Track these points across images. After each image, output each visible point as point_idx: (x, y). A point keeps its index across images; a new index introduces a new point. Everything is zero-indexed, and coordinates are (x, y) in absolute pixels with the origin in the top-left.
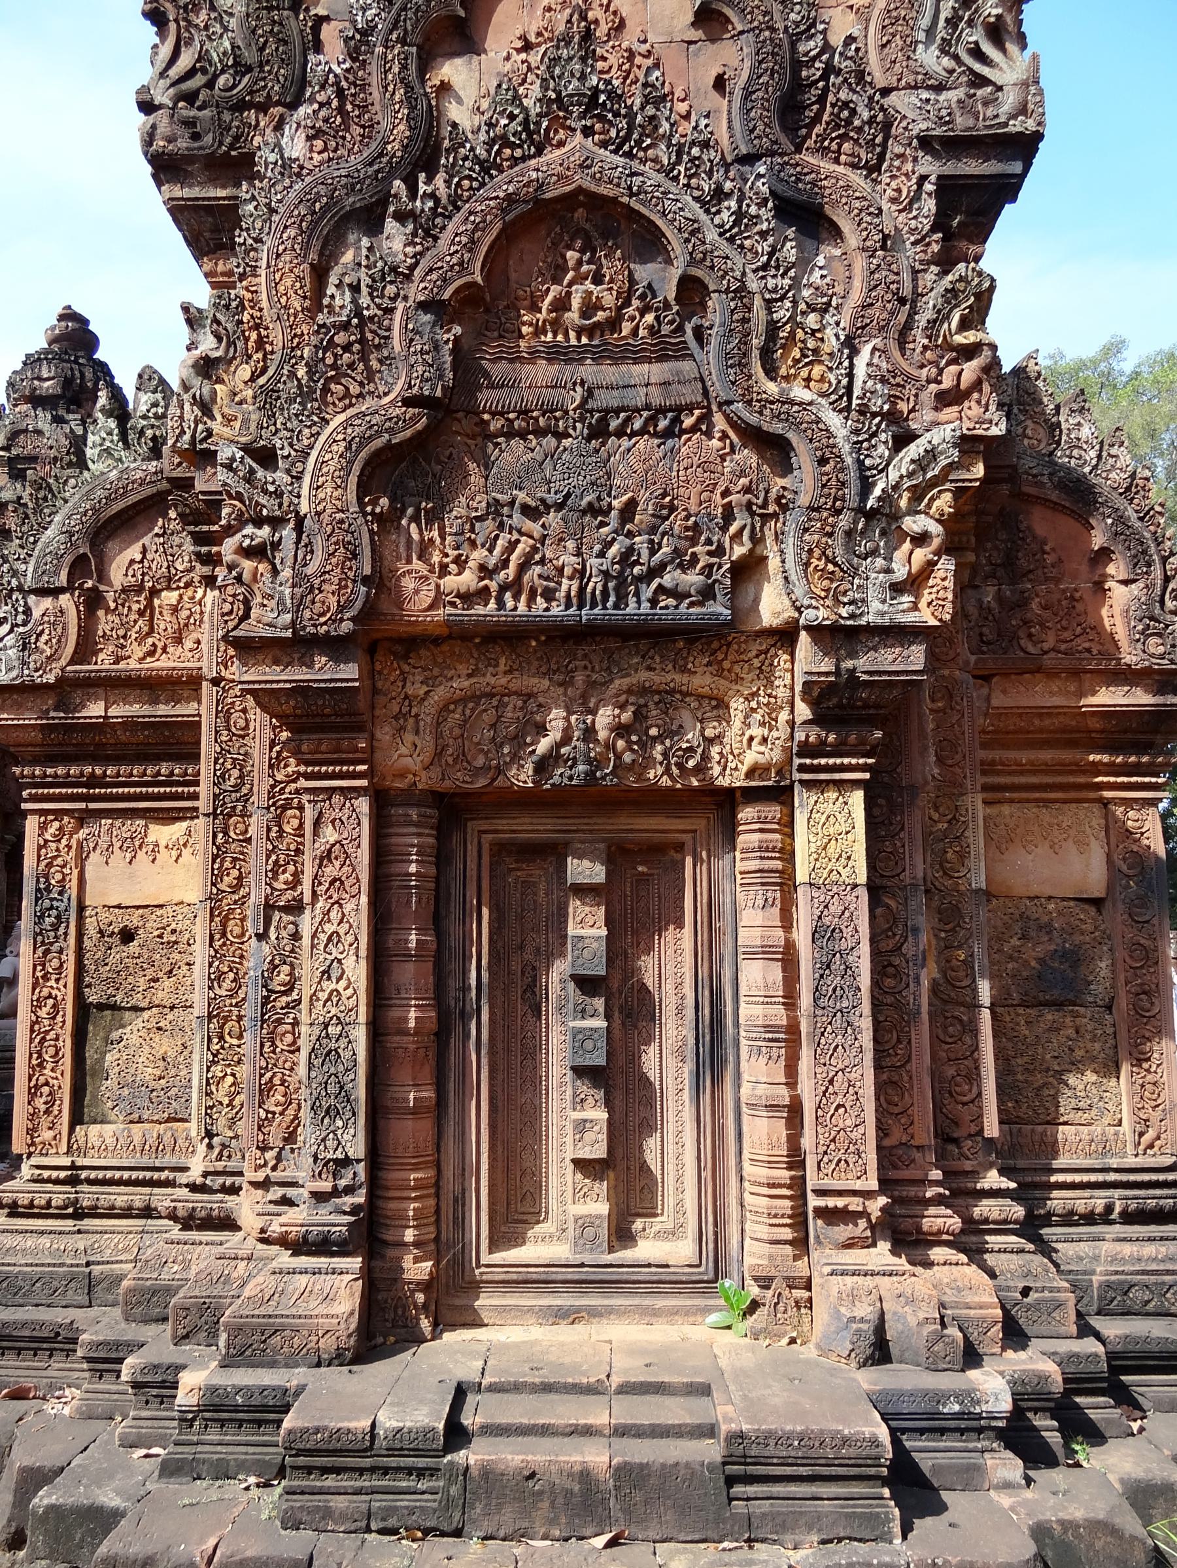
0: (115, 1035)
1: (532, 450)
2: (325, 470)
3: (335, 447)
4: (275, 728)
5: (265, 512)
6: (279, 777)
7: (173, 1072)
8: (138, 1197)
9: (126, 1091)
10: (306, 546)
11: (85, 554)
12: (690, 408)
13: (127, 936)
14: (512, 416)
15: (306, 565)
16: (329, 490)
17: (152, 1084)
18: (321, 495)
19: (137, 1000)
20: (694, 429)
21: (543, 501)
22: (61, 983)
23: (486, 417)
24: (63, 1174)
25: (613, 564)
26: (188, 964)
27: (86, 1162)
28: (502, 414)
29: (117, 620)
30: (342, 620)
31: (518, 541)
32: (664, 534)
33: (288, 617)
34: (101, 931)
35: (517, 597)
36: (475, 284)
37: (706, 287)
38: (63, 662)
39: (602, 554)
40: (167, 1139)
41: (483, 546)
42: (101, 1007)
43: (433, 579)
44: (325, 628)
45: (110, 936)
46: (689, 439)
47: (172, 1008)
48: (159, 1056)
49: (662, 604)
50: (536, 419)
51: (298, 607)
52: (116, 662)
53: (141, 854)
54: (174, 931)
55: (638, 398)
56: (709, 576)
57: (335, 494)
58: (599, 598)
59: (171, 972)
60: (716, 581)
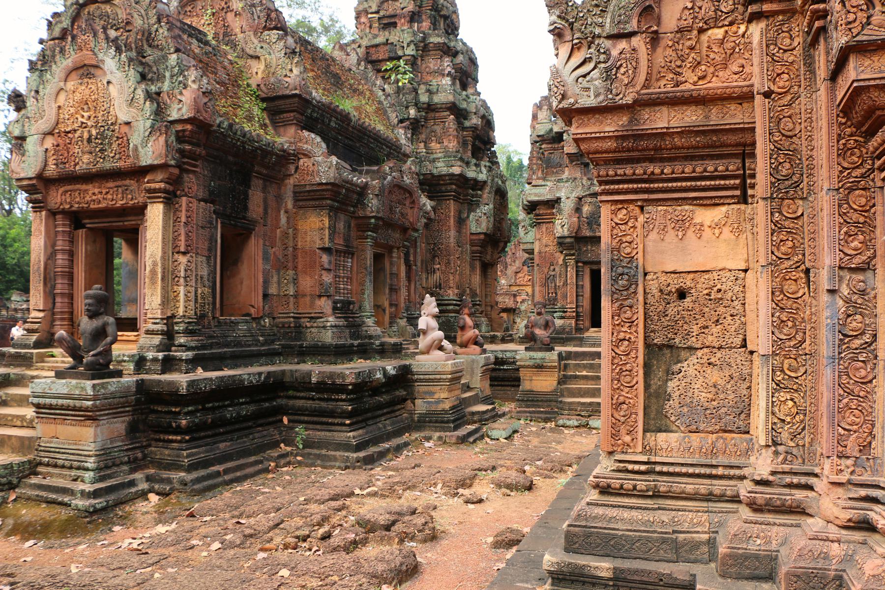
0: (676, 368)
4: (841, 124)
6: (846, 165)
7: (722, 396)
8: (703, 486)
9: (686, 409)
11: (650, 6)
13: (682, 294)
17: (706, 404)
19: (692, 342)
22: (634, 329)
24: (643, 468)
26: (732, 316)
27: (658, 459)
29: (674, 54)
34: (661, 291)
38: (638, 88)
40: (720, 444)
42: (661, 347)
45: (668, 294)
47: (719, 348)
48: (710, 384)
52: (677, 85)
53: (690, 233)
54: (719, 291)
59: (717, 321)
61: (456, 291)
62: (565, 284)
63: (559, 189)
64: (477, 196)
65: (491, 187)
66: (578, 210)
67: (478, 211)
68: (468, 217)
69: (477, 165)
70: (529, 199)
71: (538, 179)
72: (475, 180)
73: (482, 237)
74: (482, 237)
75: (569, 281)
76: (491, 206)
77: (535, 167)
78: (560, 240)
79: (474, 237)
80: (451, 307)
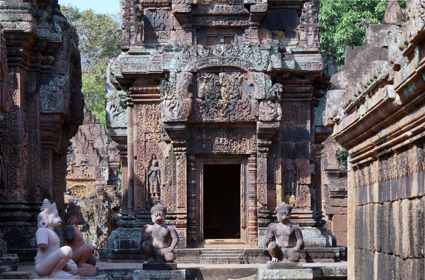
61: (24, 191)
62: (173, 183)
63: (167, 60)
64: (47, 62)
65: (68, 51)
66: (192, 88)
67: (51, 83)
68: (37, 90)
69: (50, 20)
70: (125, 71)
71: (137, 44)
72: (50, 43)
73: (57, 118)
74: (57, 118)
75: (178, 179)
76: (68, 77)
77: (133, 28)
78: (169, 127)
79: (45, 119)
80: (19, 213)
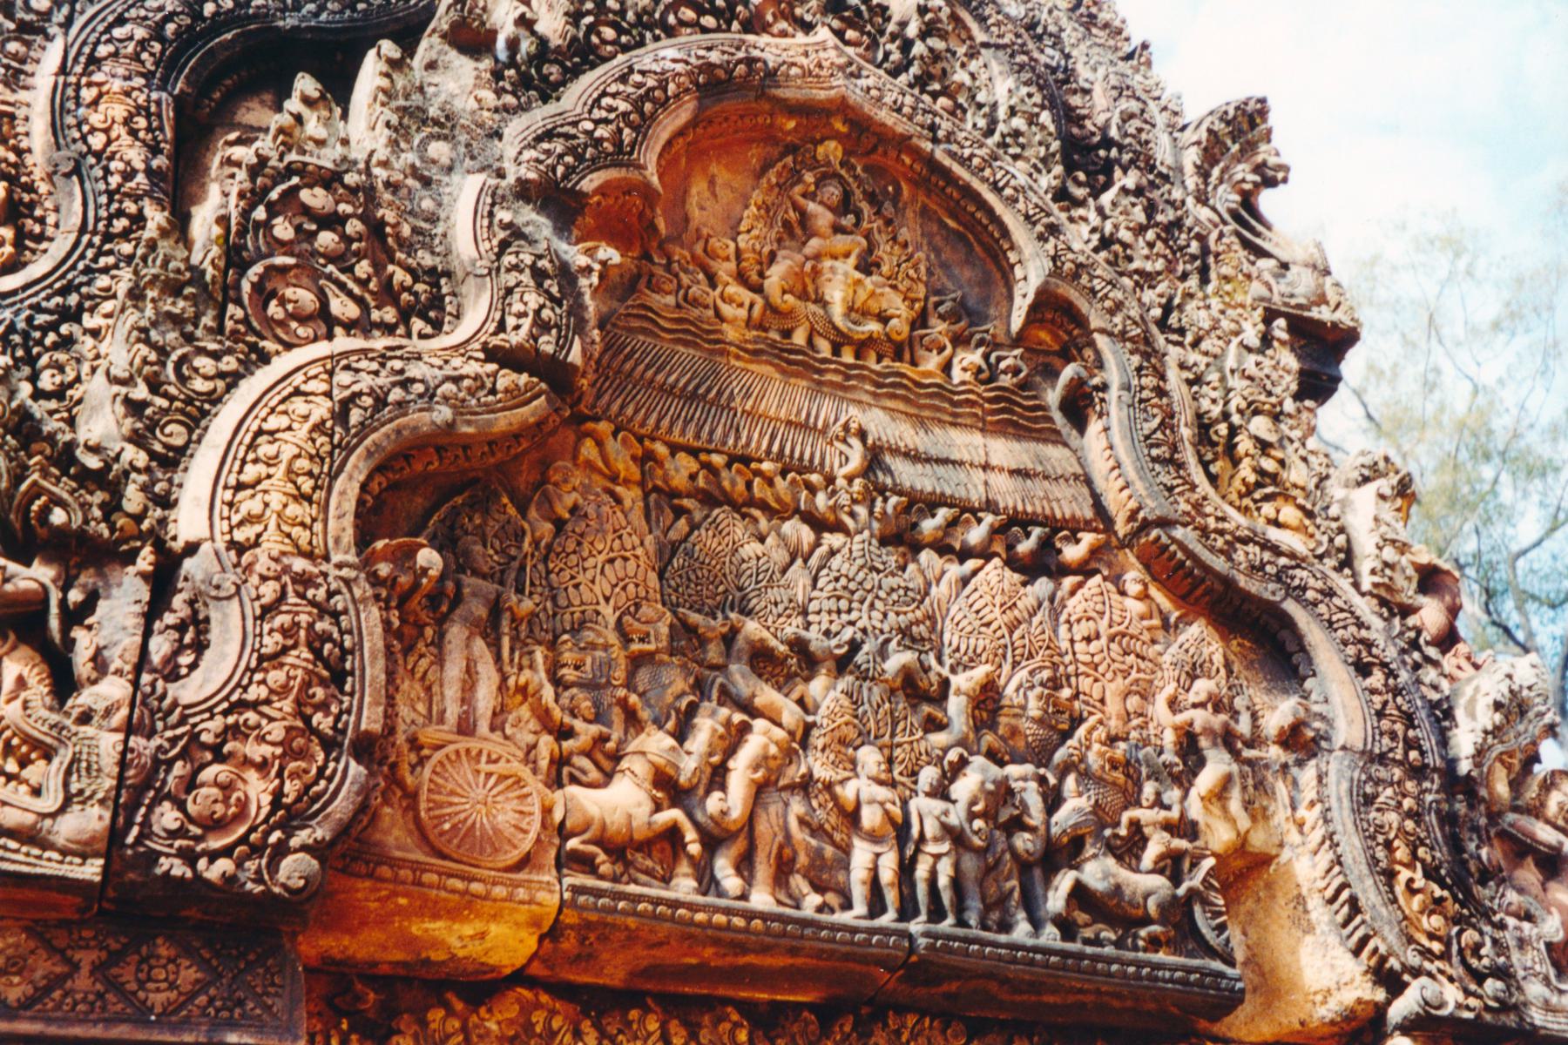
1: (762, 540)
2: (265, 449)
3: (299, 405)
5: (58, 517)
10: (181, 628)
12: (1074, 528)
14: (718, 459)
15: (173, 676)
16: (276, 500)
18: (250, 505)
20: (1085, 570)
21: (799, 646)
23: (661, 449)
25: (972, 816)
28: (694, 452)
30: (282, 850)
31: (745, 729)
32: (1065, 769)
33: (90, 820)
35: (744, 866)
36: (646, 190)
37: (1080, 321)
39: (941, 792)
41: (659, 724)
43: (534, 785)
44: (225, 865)
46: (1080, 585)
49: (1088, 933)
50: (770, 482)
51: (135, 790)
55: (973, 487)
56: (1176, 880)
57: (294, 510)
58: (946, 898)
60: (1192, 892)
